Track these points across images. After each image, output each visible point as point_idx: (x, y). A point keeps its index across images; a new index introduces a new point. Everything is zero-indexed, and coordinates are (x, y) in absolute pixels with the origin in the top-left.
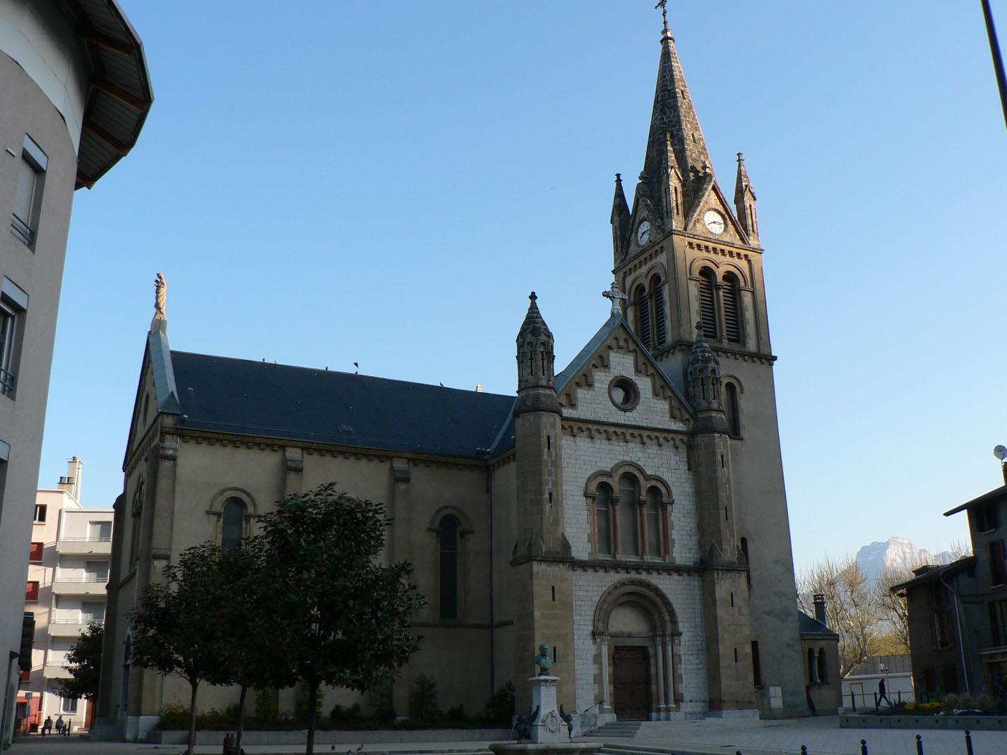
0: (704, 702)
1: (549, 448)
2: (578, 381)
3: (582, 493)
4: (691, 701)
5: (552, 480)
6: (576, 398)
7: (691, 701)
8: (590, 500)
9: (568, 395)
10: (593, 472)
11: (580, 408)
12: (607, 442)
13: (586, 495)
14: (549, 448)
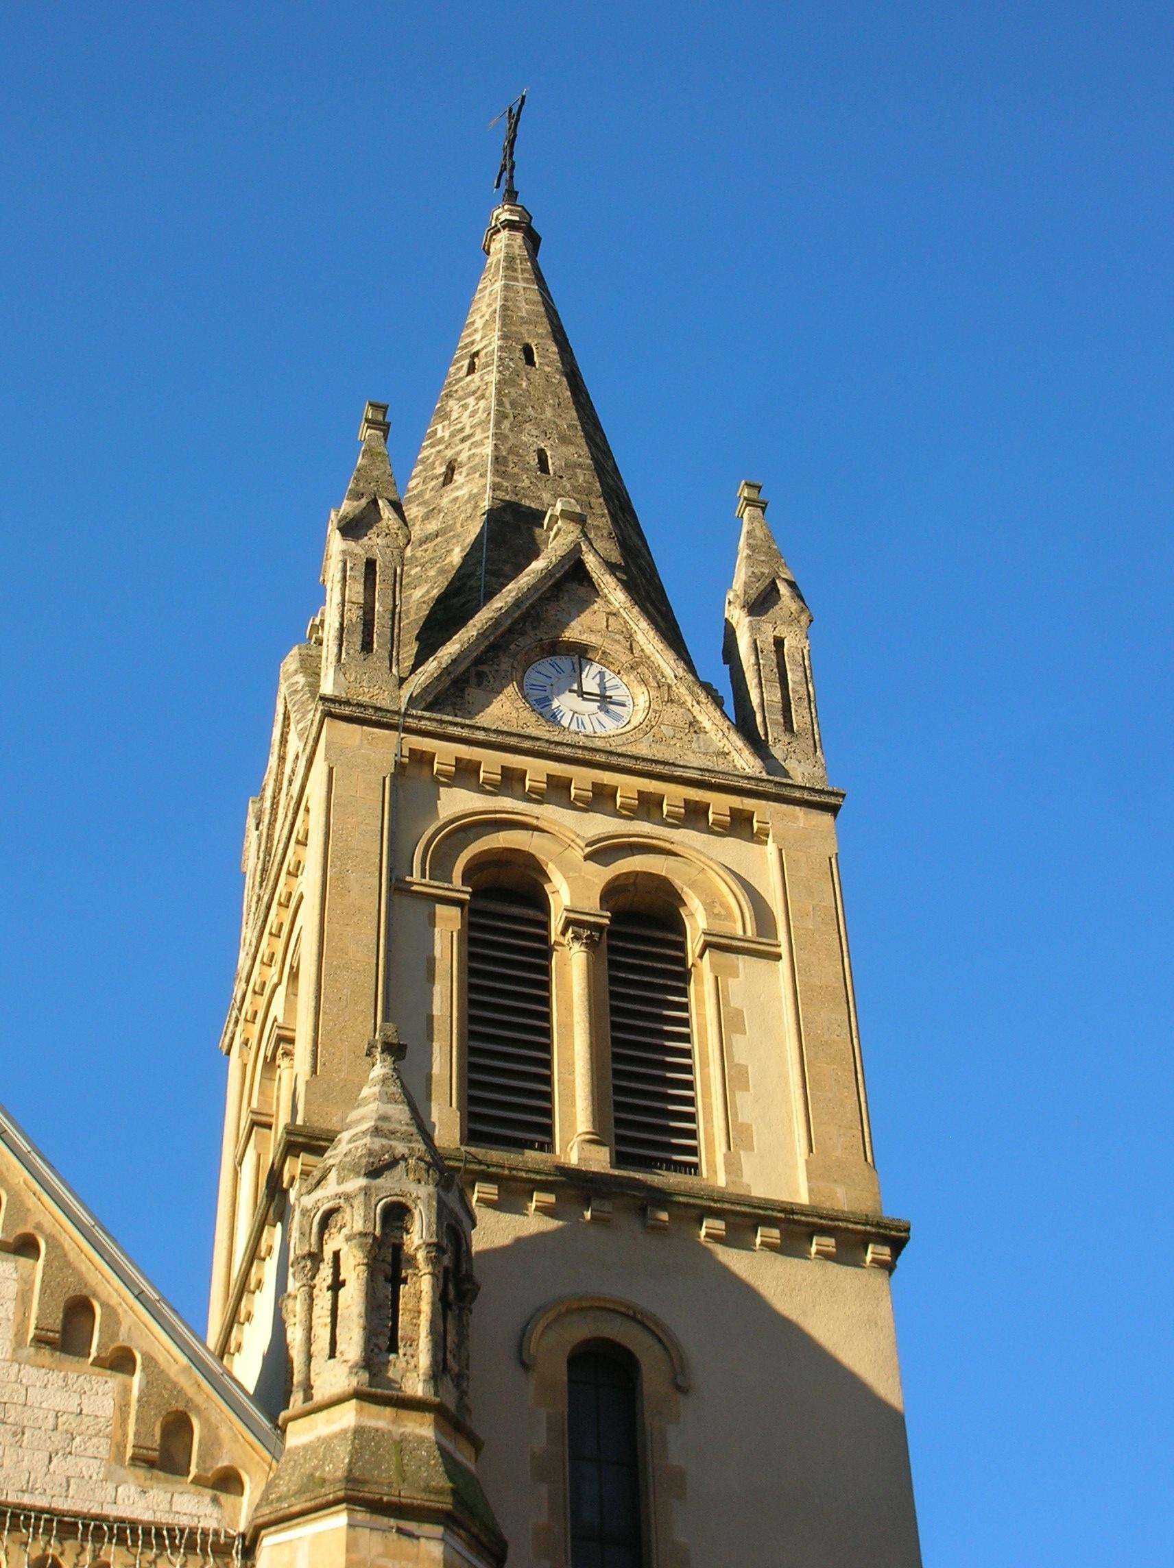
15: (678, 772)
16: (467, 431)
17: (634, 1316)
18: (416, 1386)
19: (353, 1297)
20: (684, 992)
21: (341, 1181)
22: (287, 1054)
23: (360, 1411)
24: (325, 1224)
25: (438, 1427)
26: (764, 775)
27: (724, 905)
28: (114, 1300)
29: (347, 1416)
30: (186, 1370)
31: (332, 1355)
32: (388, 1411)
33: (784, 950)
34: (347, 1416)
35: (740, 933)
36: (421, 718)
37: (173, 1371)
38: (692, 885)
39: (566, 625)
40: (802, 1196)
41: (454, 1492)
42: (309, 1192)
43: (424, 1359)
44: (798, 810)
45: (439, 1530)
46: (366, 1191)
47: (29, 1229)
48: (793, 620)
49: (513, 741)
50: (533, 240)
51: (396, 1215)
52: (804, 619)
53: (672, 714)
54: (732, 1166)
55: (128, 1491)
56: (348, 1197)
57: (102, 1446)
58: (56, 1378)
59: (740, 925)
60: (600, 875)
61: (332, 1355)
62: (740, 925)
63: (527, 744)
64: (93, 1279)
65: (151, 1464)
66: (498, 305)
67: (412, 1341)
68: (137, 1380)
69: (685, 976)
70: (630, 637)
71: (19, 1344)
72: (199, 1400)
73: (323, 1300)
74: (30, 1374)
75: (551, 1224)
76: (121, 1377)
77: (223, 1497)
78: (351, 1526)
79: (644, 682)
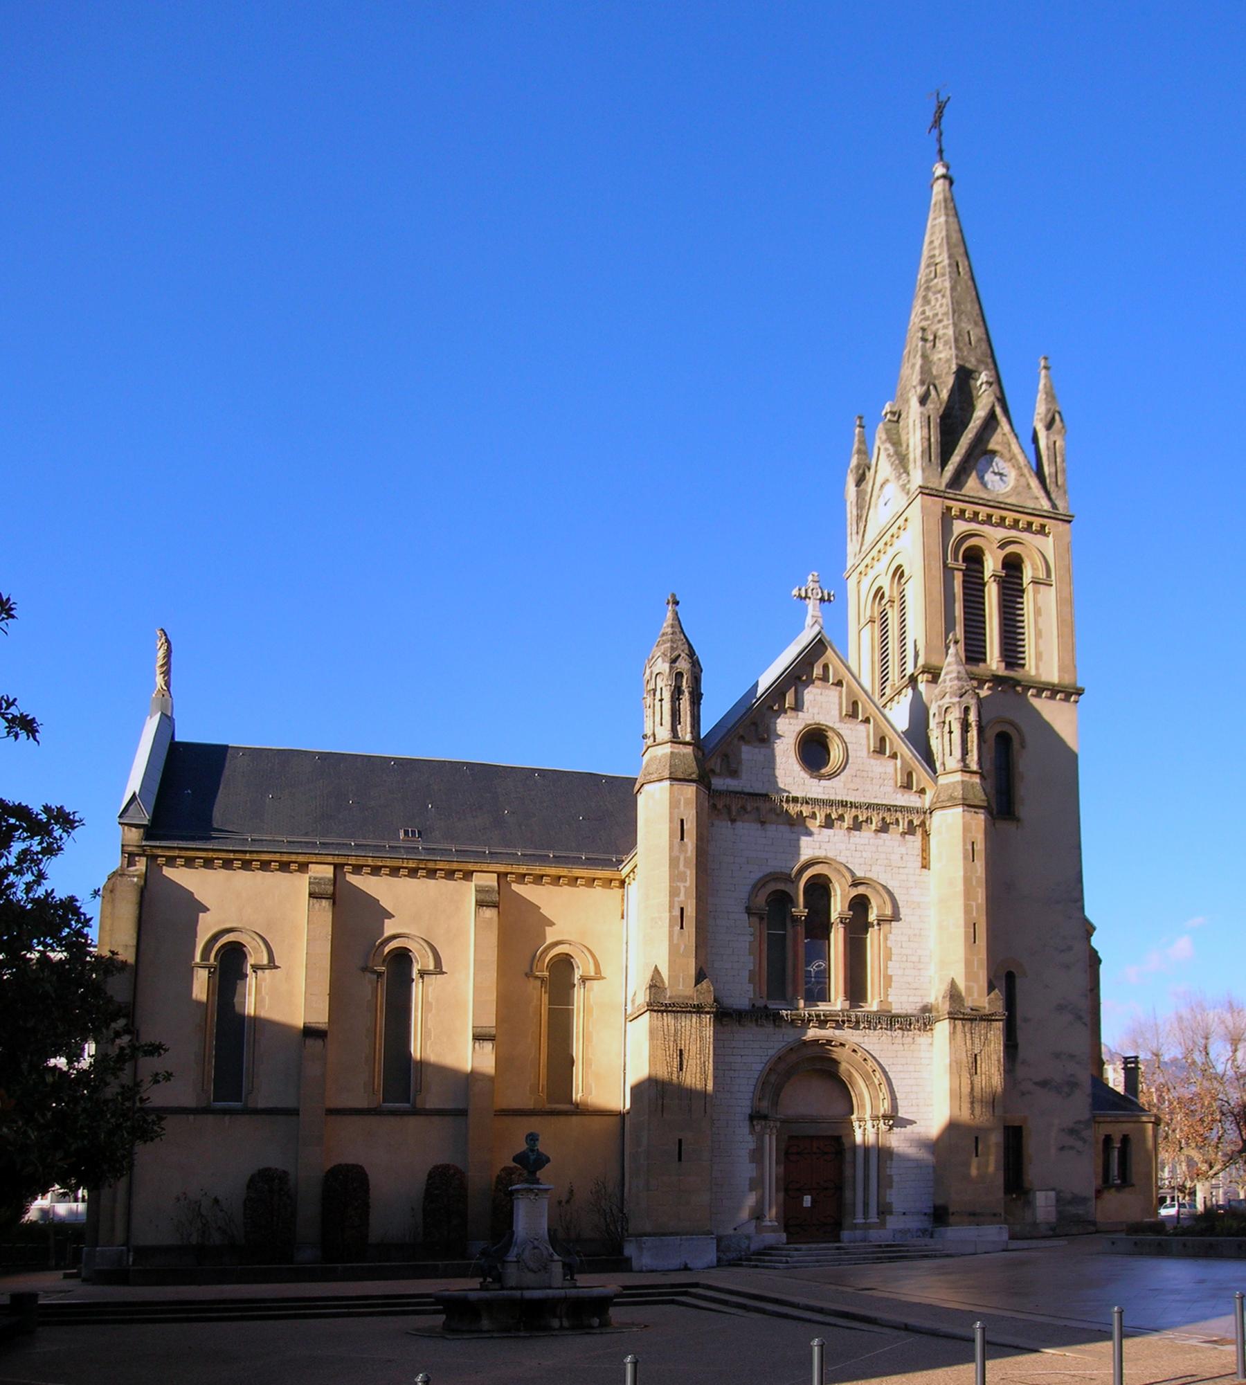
0: (925, 1214)
1: (682, 839)
3: (742, 909)
4: (904, 1214)
5: (684, 886)
6: (740, 762)
7: (904, 1214)
8: (755, 920)
9: (726, 757)
10: (761, 875)
11: (744, 776)
12: (788, 827)
13: (749, 911)
14: (682, 839)
15: (1026, 510)
16: (940, 317)
17: (1012, 724)
18: (974, 767)
20: (1022, 597)
21: (951, 698)
23: (962, 775)
24: (946, 711)
25: (981, 779)
26: (1051, 510)
27: (1037, 565)
28: (891, 737)
29: (958, 777)
30: (911, 758)
31: (951, 755)
32: (968, 775)
33: (1054, 583)
35: (1041, 577)
36: (949, 493)
37: (908, 758)
38: (1028, 557)
39: (988, 441)
40: (1055, 680)
41: (987, 800)
42: (941, 699)
43: (975, 757)
44: (1060, 523)
45: (982, 811)
46: (959, 702)
47: (868, 715)
48: (1059, 432)
49: (976, 500)
50: (951, 183)
51: (967, 709)
52: (1063, 431)
53: (1023, 481)
54: (1037, 668)
55: (899, 796)
56: (954, 704)
57: (892, 782)
58: (879, 762)
59: (1042, 575)
60: (1001, 554)
61: (951, 755)
62: (1042, 575)
63: (981, 502)
64: (886, 731)
65: (904, 787)
66: (944, 233)
67: (972, 751)
68: (899, 761)
69: (1023, 591)
70: (1009, 445)
71: (869, 752)
72: (914, 767)
73: (947, 736)
74: (873, 762)
75: (990, 692)
76: (894, 761)
77: (922, 796)
78: (964, 811)
79: (1014, 466)
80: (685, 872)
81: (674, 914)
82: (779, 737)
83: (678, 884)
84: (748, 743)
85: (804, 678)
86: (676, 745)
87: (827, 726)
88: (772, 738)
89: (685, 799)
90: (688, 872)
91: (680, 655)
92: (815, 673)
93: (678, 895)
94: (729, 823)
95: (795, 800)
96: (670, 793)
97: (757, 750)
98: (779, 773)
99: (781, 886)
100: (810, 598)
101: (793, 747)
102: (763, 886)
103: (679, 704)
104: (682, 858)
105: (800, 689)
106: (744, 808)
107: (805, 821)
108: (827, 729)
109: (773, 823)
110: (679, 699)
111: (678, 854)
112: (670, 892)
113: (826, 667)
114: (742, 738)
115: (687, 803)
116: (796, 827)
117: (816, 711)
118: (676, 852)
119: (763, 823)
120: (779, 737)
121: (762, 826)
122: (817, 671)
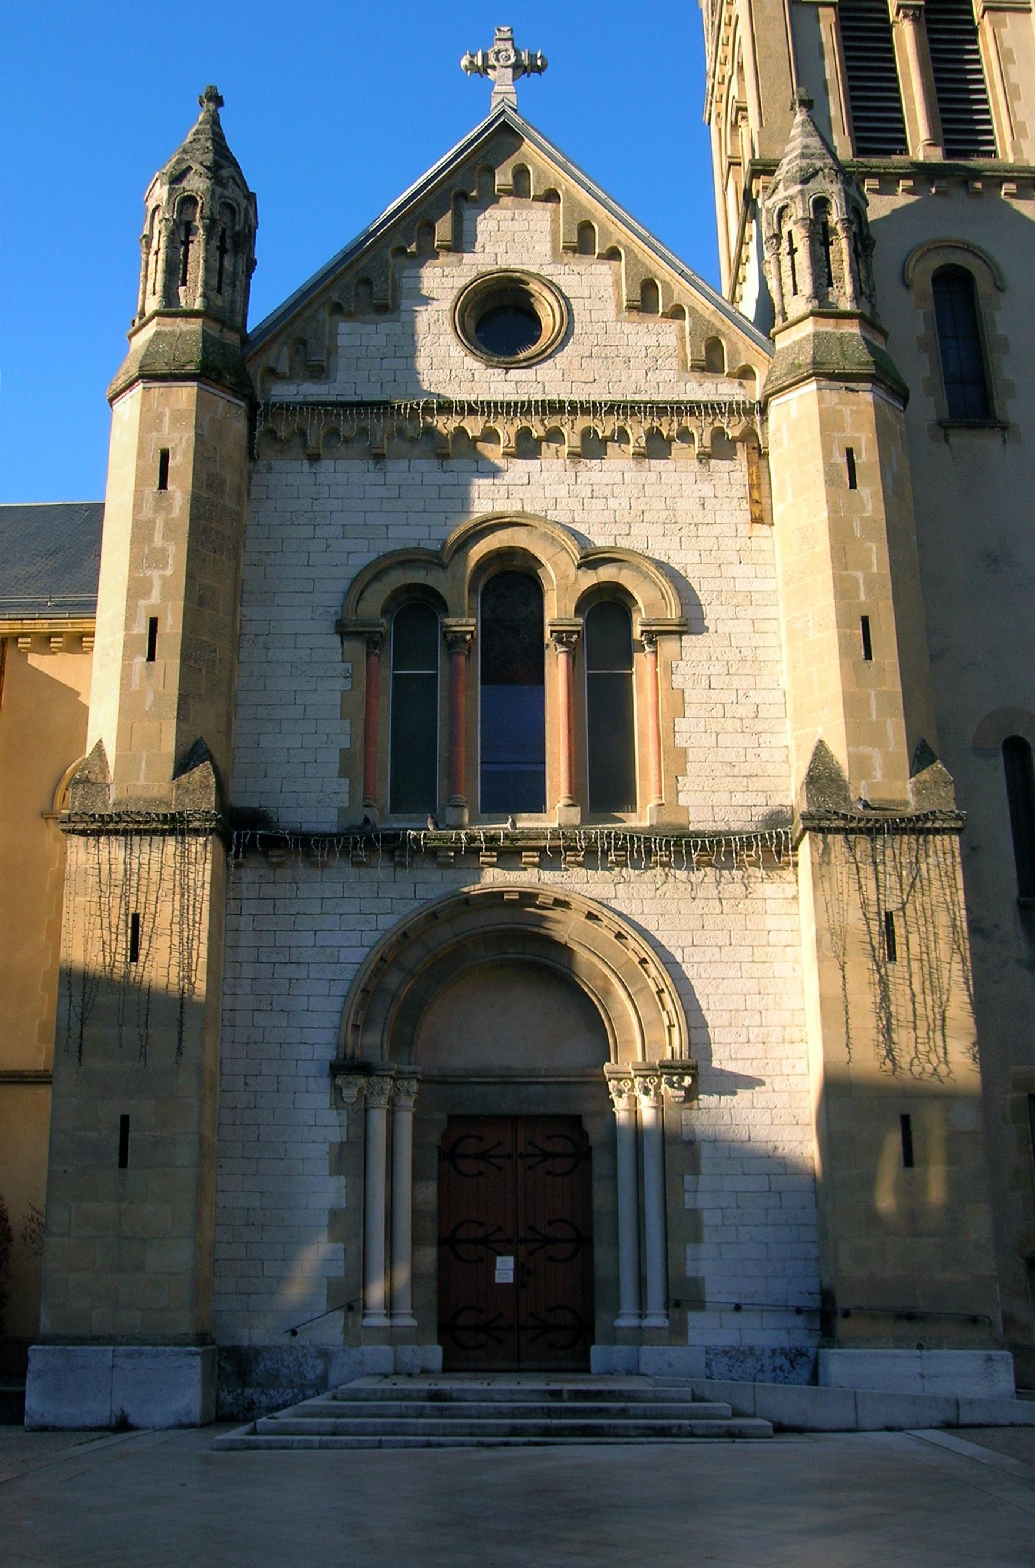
0: (798, 1311)
1: (163, 485)
2: (335, 299)
3: (328, 626)
4: (738, 1308)
6: (332, 351)
7: (738, 1308)
8: (358, 648)
10: (373, 556)
11: (341, 375)
12: (435, 463)
13: (343, 630)
14: (163, 485)
18: (846, 305)
19: (803, 257)
20: (975, 42)
21: (786, 189)
22: (743, 118)
23: (815, 323)
24: (780, 216)
28: (668, 278)
29: (808, 327)
30: (714, 313)
31: (795, 293)
34: (808, 327)
37: (707, 315)
42: (769, 198)
43: (849, 289)
45: (869, 386)
46: (802, 192)
47: (614, 244)
51: (821, 204)
54: (1017, 149)
55: (692, 386)
56: (792, 198)
57: (674, 363)
58: (642, 327)
61: (795, 293)
64: (654, 268)
65: (702, 369)
67: (840, 279)
68: (687, 323)
69: (975, 32)
71: (619, 311)
72: (724, 329)
73: (786, 261)
74: (628, 327)
75: (912, 199)
77: (745, 382)
78: (819, 389)
80: (164, 550)
81: (135, 632)
82: (427, 300)
83: (148, 573)
84: (350, 316)
85: (474, 193)
86: (169, 320)
87: (523, 272)
88: (405, 304)
89: (173, 412)
90: (172, 548)
91: (190, 168)
92: (497, 183)
93: (147, 594)
94: (306, 463)
95: (445, 407)
96: (143, 405)
97: (370, 328)
98: (422, 363)
99: (417, 576)
100: (494, 68)
101: (449, 315)
102: (378, 577)
103: (187, 251)
104: (160, 523)
105: (467, 214)
106: (334, 433)
107: (475, 447)
108: (525, 278)
109: (404, 457)
110: (187, 243)
111: (151, 515)
112: (129, 590)
113: (521, 172)
114: (337, 308)
115: (177, 419)
116: (452, 462)
117: (501, 248)
118: (148, 513)
119: (379, 458)
120: (427, 300)
121: (376, 464)
122: (503, 177)
